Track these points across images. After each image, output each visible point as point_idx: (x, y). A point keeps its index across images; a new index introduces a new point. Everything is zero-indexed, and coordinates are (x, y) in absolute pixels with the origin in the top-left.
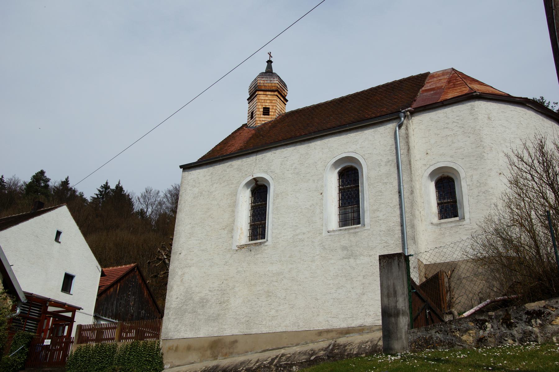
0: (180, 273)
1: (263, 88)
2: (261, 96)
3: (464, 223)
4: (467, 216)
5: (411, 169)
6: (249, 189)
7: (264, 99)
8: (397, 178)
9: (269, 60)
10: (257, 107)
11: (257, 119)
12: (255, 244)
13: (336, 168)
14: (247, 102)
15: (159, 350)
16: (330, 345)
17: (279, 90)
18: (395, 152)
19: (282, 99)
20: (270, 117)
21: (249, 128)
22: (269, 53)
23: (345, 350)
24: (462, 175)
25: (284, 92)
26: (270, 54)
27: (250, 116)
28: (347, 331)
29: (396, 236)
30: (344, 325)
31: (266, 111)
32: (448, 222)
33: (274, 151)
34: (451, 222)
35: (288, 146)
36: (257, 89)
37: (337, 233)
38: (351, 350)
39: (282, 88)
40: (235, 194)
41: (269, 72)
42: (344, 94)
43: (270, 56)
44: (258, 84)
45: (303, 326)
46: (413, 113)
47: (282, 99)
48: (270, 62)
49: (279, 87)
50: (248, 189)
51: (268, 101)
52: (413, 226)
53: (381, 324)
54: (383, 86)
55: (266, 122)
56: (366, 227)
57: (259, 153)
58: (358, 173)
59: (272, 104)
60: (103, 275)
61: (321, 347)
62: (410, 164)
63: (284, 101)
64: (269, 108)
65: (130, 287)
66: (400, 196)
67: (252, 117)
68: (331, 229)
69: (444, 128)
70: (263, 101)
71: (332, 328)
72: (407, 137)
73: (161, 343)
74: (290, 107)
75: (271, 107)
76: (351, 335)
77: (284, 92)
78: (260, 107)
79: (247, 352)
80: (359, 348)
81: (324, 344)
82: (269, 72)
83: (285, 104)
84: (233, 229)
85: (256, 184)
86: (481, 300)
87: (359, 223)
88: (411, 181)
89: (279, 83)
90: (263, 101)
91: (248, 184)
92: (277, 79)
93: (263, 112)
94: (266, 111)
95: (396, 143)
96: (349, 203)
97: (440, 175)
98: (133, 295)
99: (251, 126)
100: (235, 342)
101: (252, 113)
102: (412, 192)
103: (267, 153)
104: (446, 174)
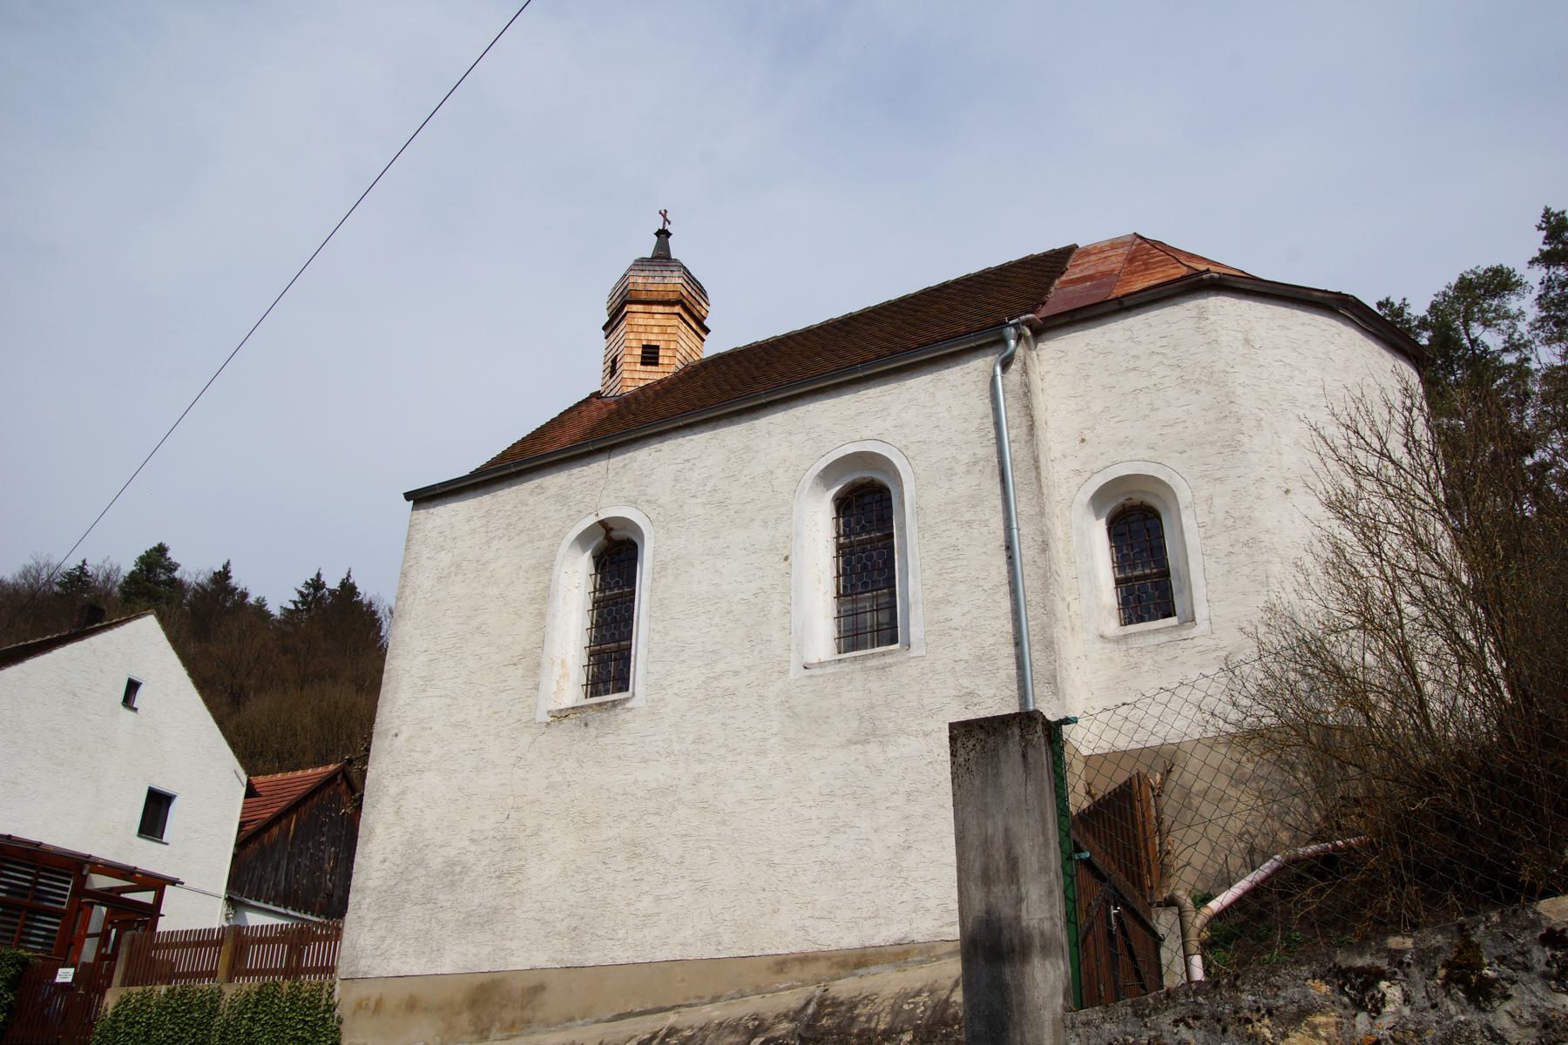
0: (393, 790)
1: (643, 296)
2: (638, 316)
3: (1195, 632)
4: (1201, 611)
5: (1039, 480)
6: (589, 553)
7: (646, 325)
8: (1000, 508)
9: (661, 228)
10: (627, 343)
11: (625, 375)
12: (600, 704)
13: (828, 487)
14: (603, 333)
15: (331, 1008)
16: (808, 1003)
17: (685, 301)
18: (992, 435)
19: (694, 326)
20: (660, 369)
21: (606, 400)
22: (663, 212)
23: (853, 1019)
24: (1184, 495)
25: (698, 307)
26: (664, 214)
27: (609, 369)
28: (859, 960)
29: (1002, 674)
30: (850, 940)
31: (650, 355)
32: (1149, 632)
33: (655, 446)
34: (1158, 630)
35: (696, 430)
36: (627, 298)
37: (830, 670)
38: (869, 1020)
39: (694, 298)
40: (546, 566)
41: (662, 256)
42: (855, 306)
43: (666, 220)
44: (630, 287)
45: (731, 946)
46: (1040, 331)
47: (694, 326)
48: (663, 234)
49: (685, 293)
50: (584, 551)
51: (656, 330)
52: (1050, 646)
53: (958, 937)
54: (957, 282)
55: (650, 382)
56: (915, 652)
57: (618, 451)
58: (890, 499)
59: (666, 337)
60: (251, 792)
61: (781, 1009)
62: (1037, 468)
63: (699, 331)
64: (657, 347)
65: (324, 824)
66: (1011, 559)
67: (613, 371)
68: (812, 658)
69: (1128, 370)
70: (642, 329)
71: (816, 948)
72: (1027, 391)
73: (338, 988)
74: (715, 345)
75: (662, 345)
76: (873, 969)
77: (698, 307)
78: (634, 344)
79: (571, 1019)
80: (896, 1011)
81: (790, 1000)
82: (662, 256)
83: (703, 340)
84: (539, 665)
85: (608, 537)
86: (1252, 859)
87: (894, 640)
88: (1042, 514)
89: (685, 285)
90: (642, 329)
91: (583, 539)
92: (681, 274)
93: (643, 358)
94: (650, 355)
95: (996, 409)
96: (865, 584)
97: (1121, 500)
98: (333, 844)
99: (611, 394)
100: (539, 989)
101: (614, 362)
102: (1045, 547)
103: (638, 452)
104: (1137, 498)
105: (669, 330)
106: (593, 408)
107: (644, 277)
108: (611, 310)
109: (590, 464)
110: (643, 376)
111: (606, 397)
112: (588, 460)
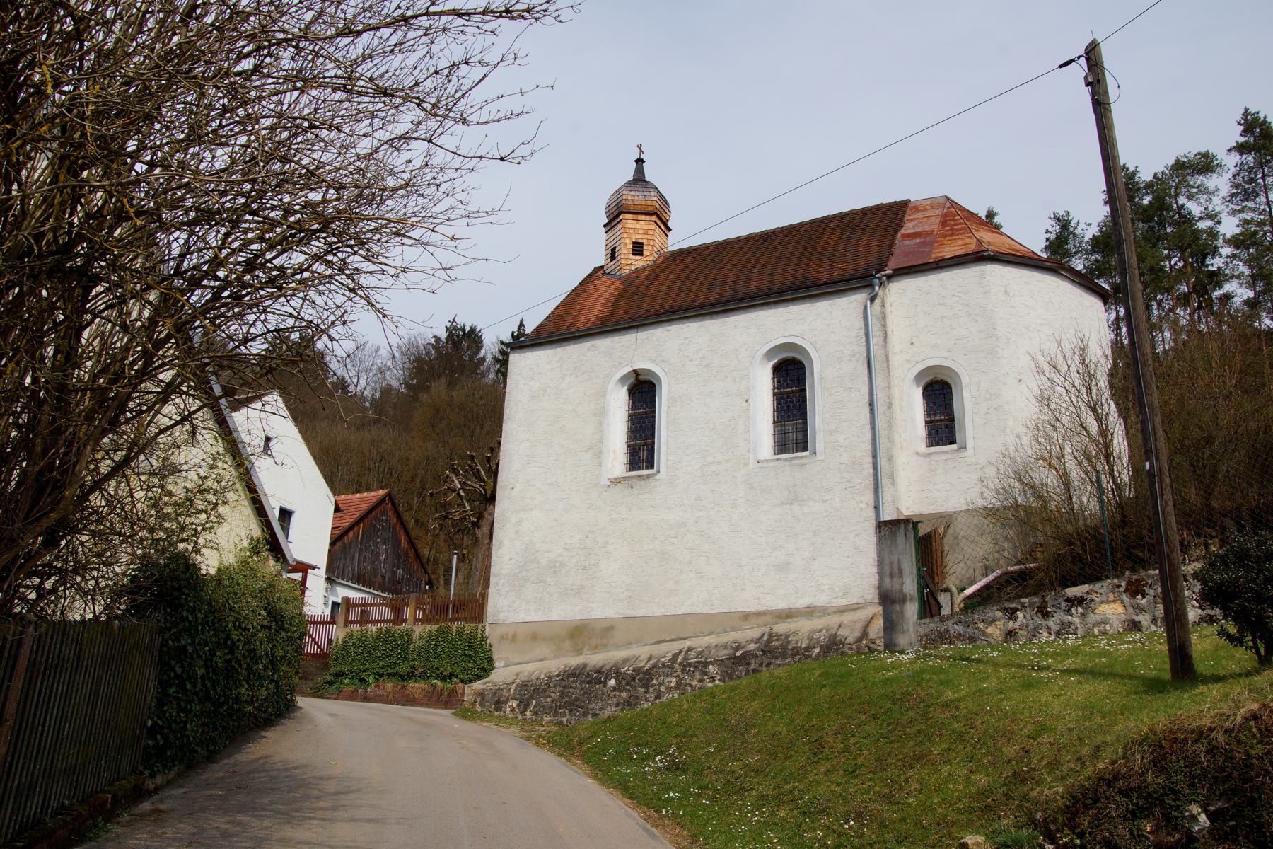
0: (513, 520)
1: (632, 209)
2: (629, 222)
3: (966, 454)
4: (970, 444)
5: (888, 367)
6: (625, 388)
7: (635, 228)
8: (867, 382)
10: (623, 240)
12: (640, 476)
13: (769, 361)
14: (604, 229)
15: (484, 639)
16: (763, 635)
18: (864, 339)
23: (788, 643)
24: (965, 379)
26: (640, 148)
28: (788, 615)
29: (865, 473)
30: (783, 605)
31: (638, 249)
32: (942, 452)
34: (947, 452)
37: (772, 464)
38: (797, 642)
40: (602, 394)
41: (639, 180)
42: (770, 226)
43: (641, 151)
44: (624, 202)
45: (718, 607)
46: (889, 277)
48: (640, 161)
50: (623, 386)
51: (641, 232)
52: (891, 459)
54: (835, 217)
56: (819, 457)
58: (804, 368)
60: (337, 509)
61: (749, 638)
62: (888, 361)
64: (642, 243)
65: (379, 530)
66: (872, 410)
67: (613, 257)
68: (762, 458)
69: (939, 304)
70: (632, 231)
71: (764, 609)
72: (883, 317)
73: (487, 628)
75: (645, 242)
76: (795, 619)
78: (628, 241)
79: (630, 644)
80: (810, 639)
81: (754, 633)
82: (639, 180)
84: (601, 452)
85: (637, 379)
86: (987, 570)
87: (805, 449)
88: (889, 388)
91: (623, 380)
94: (638, 249)
95: (866, 325)
96: (789, 417)
97: (931, 378)
98: (385, 543)
100: (611, 628)
101: (613, 250)
102: (890, 406)
104: (940, 377)
112: (623, 332)
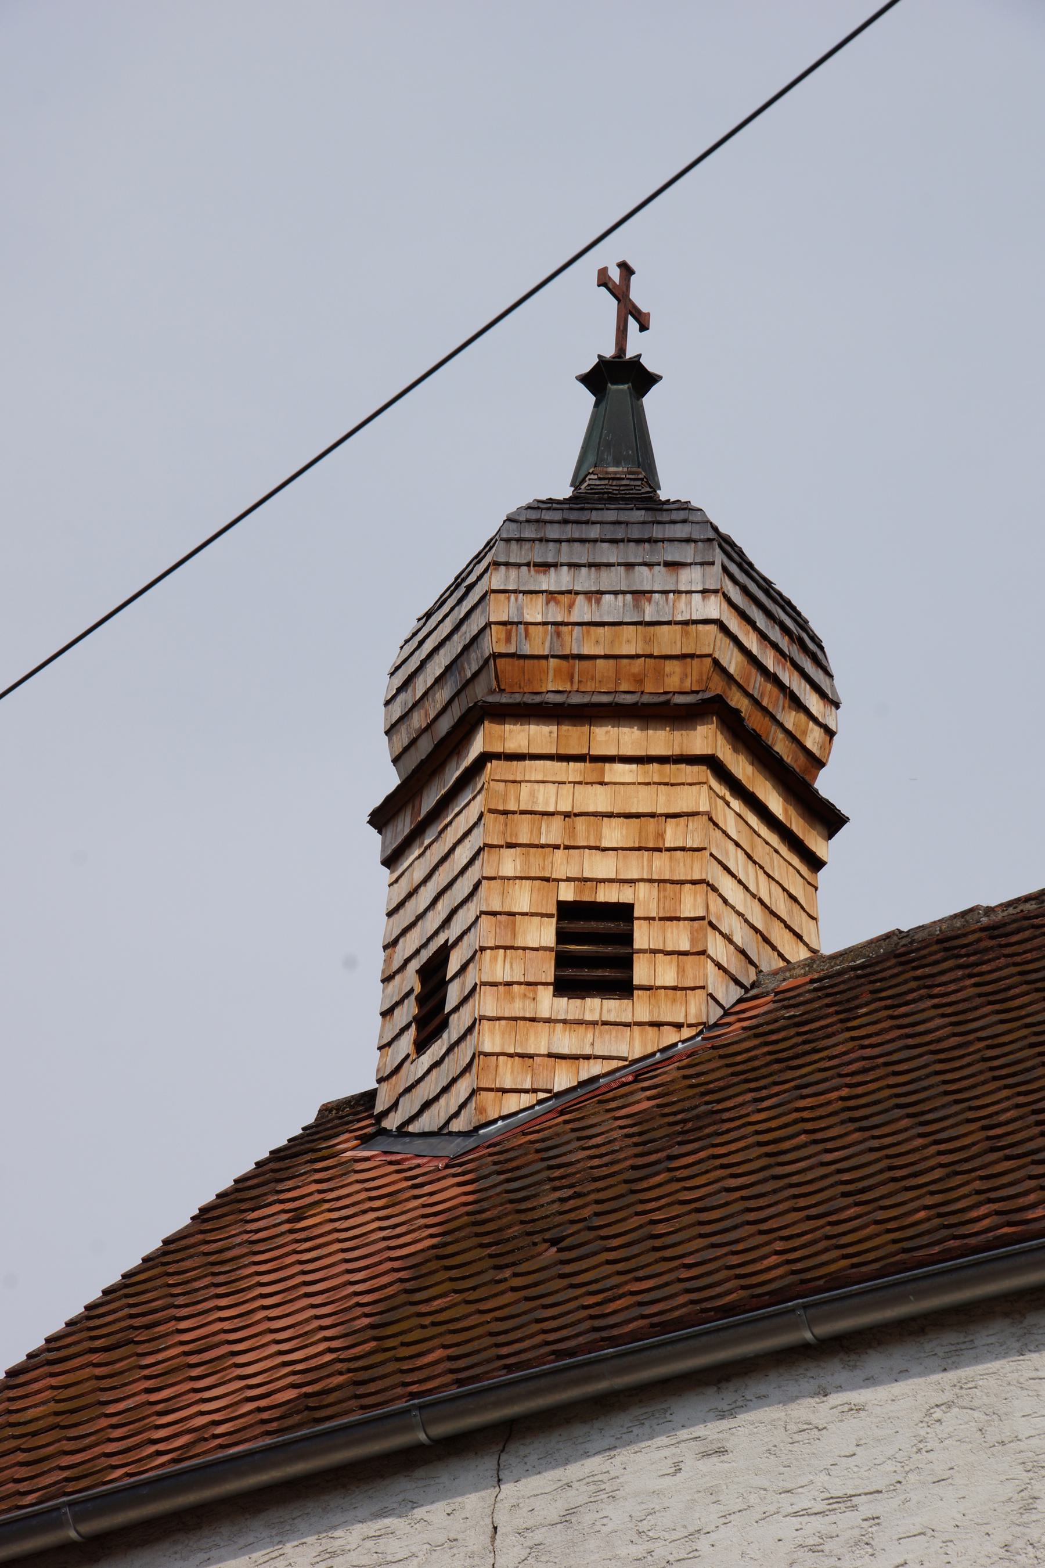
10: (490, 898)
11: (490, 1040)
14: (373, 842)
17: (737, 701)
19: (776, 804)
20: (640, 1008)
21: (403, 1148)
22: (615, 274)
25: (791, 719)
27: (409, 1010)
33: (700, 1430)
35: (875, 1362)
36: (480, 691)
39: (775, 679)
44: (494, 642)
47: (776, 804)
49: (733, 662)
51: (614, 834)
55: (596, 1068)
57: (533, 1449)
59: (661, 866)
63: (797, 825)
64: (624, 912)
70: (552, 832)
77: (791, 719)
78: (522, 898)
83: (815, 863)
89: (734, 624)
90: (552, 832)
92: (714, 577)
93: (562, 960)
99: (428, 1122)
103: (623, 1456)
105: (673, 834)
106: (352, 1189)
107: (551, 595)
108: (403, 737)
109: (415, 1504)
110: (565, 1042)
111: (402, 1132)
112: (403, 1486)
